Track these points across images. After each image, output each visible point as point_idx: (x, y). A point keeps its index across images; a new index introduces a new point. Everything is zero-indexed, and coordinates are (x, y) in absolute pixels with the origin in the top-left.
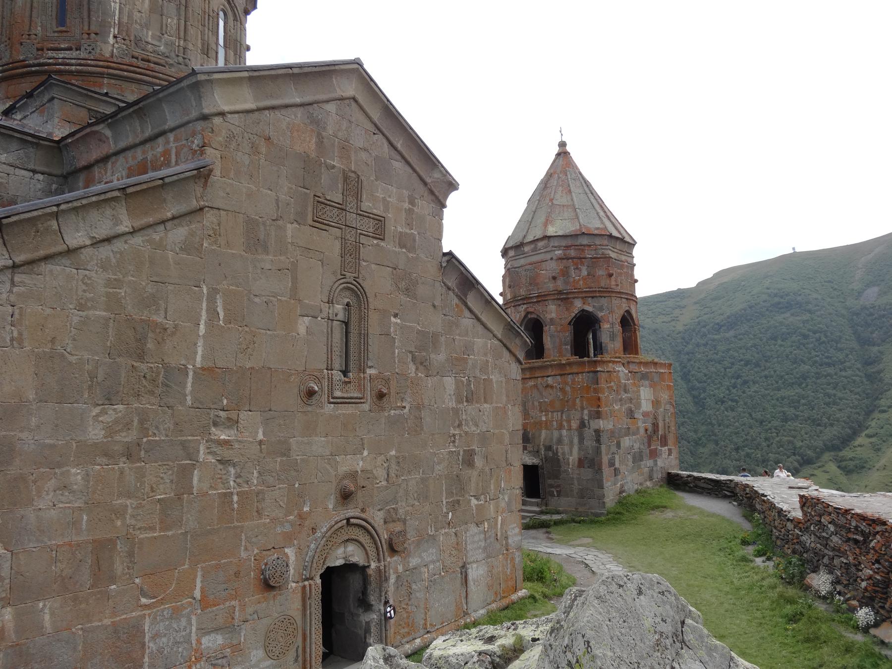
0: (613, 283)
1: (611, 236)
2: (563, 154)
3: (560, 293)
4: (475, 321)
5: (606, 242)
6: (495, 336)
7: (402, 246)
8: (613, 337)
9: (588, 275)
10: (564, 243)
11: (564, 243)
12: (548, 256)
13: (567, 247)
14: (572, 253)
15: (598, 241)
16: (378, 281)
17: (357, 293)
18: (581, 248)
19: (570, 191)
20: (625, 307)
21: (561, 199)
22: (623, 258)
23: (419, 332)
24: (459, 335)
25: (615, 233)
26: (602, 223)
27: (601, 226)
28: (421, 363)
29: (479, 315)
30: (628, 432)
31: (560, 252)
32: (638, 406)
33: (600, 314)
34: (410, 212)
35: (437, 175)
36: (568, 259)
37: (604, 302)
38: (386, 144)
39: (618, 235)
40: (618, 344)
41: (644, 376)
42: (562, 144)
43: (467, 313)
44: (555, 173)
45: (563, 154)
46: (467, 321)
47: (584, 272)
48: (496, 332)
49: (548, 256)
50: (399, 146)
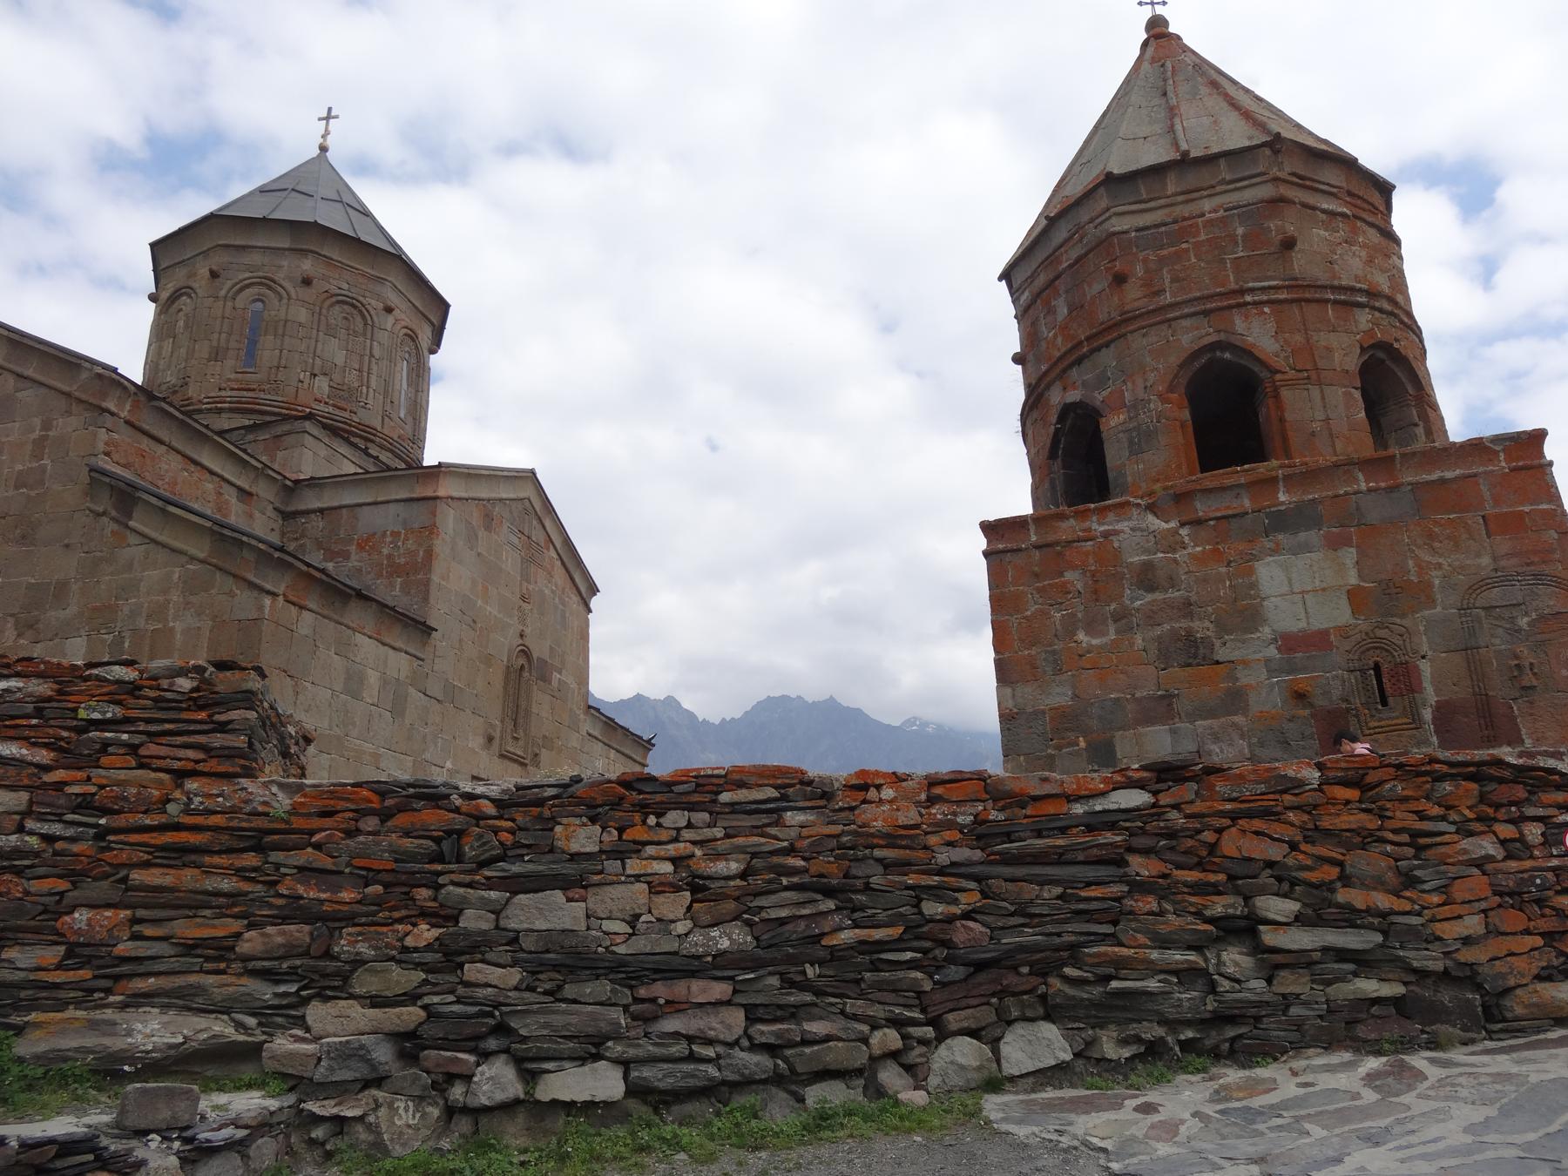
4: (152, 546)
6: (193, 559)
7: (16, 488)
8: (1140, 441)
9: (1070, 312)
13: (1033, 277)
14: (1042, 279)
15: (1084, 215)
23: (30, 586)
24: (112, 574)
28: (31, 627)
29: (153, 534)
30: (1162, 708)
31: (1027, 294)
33: (1098, 397)
34: (44, 438)
35: (84, 375)
37: (1108, 358)
38: (11, 380)
41: (1281, 522)
43: (133, 539)
46: (135, 551)
47: (1063, 311)
48: (193, 551)
50: (29, 372)
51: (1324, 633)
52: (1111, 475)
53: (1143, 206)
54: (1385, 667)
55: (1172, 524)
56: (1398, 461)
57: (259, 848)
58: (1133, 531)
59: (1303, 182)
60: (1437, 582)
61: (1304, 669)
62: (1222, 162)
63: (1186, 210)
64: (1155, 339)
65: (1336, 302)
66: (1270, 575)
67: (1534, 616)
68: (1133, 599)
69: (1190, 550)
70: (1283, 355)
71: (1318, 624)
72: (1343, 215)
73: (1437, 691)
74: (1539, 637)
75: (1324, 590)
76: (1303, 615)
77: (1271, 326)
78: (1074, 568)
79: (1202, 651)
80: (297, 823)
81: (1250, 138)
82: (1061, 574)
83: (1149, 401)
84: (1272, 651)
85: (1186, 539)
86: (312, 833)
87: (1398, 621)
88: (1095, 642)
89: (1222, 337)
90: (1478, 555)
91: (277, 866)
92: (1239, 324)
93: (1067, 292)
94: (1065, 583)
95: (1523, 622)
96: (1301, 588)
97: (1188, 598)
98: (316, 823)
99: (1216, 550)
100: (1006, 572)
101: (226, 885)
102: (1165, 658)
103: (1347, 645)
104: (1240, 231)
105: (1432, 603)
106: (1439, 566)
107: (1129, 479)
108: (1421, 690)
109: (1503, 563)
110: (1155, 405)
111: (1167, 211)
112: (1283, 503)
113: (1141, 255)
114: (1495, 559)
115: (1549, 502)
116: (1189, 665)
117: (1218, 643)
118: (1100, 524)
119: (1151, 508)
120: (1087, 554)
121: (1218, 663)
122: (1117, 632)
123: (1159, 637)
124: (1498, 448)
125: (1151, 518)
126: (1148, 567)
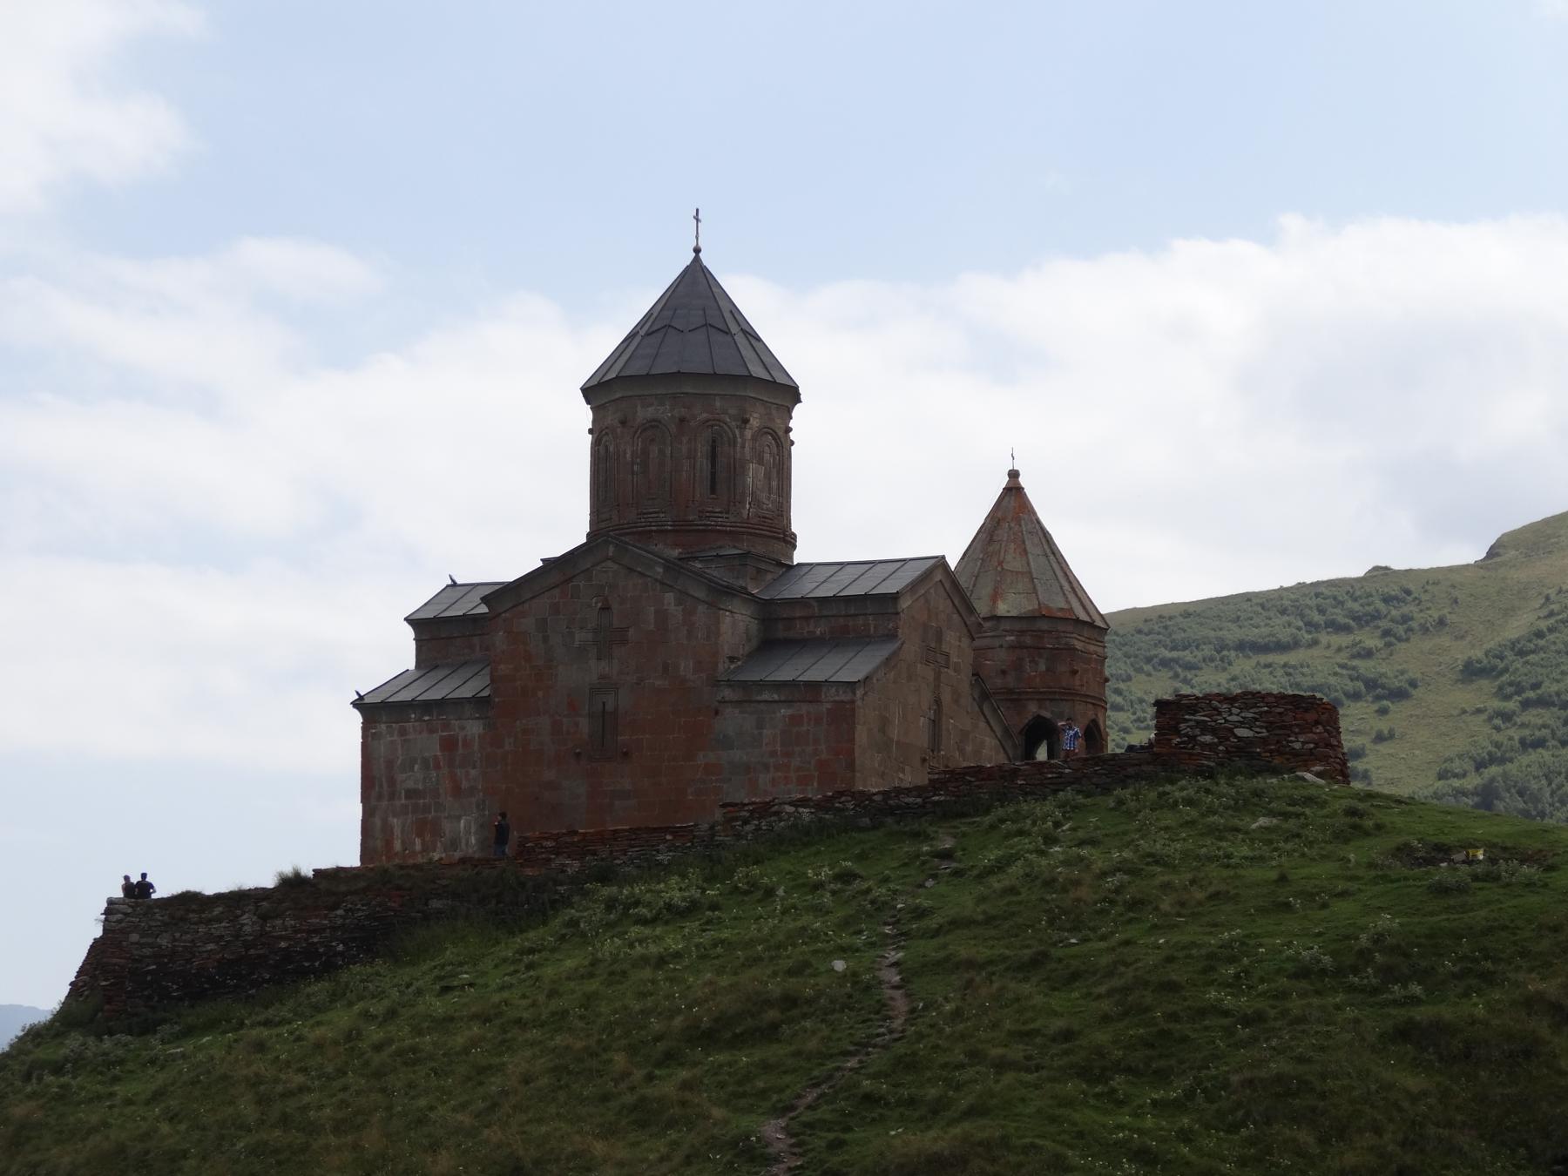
0: (1078, 683)
1: (1078, 621)
2: (1013, 490)
3: (1011, 691)
5: (1070, 628)
10: (1018, 626)
11: (1018, 626)
12: (997, 642)
13: (1022, 632)
14: (1028, 640)
16: (946, 697)
17: (938, 702)
19: (1025, 550)
20: (1091, 714)
21: (1013, 563)
22: (1092, 648)
25: (1083, 617)
26: (1068, 602)
27: (1063, 605)
36: (1022, 647)
39: (1087, 619)
42: (1014, 475)
44: (1004, 519)
45: (1013, 490)
46: (982, 724)
47: (1042, 667)
49: (997, 642)
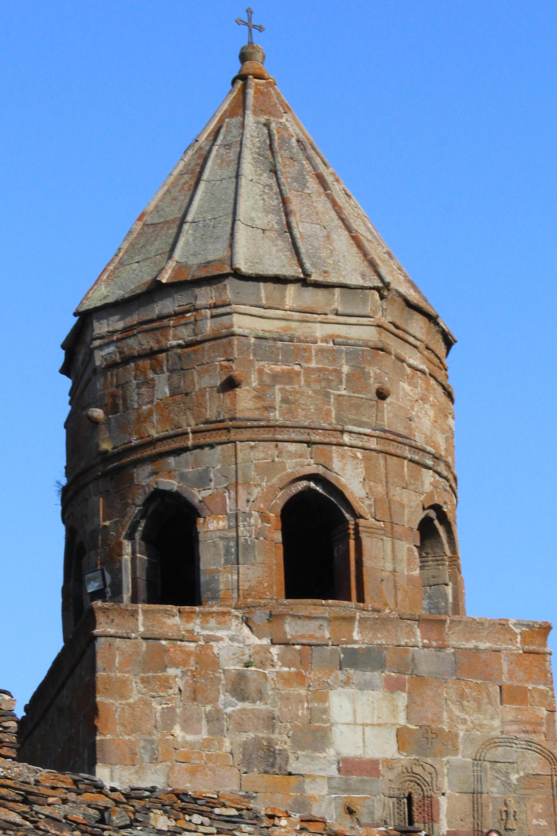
8: (236, 554)
9: (173, 395)
18: (157, 325)
32: (315, 736)
33: (198, 495)
40: (262, 569)
41: (353, 659)
51: (374, 763)
52: (203, 578)
53: (261, 311)
54: (415, 797)
55: (266, 641)
56: (447, 625)
57: (25, 801)
58: (230, 640)
59: (398, 331)
60: (461, 734)
61: (357, 791)
62: (337, 291)
63: (300, 330)
64: (262, 455)
65: (411, 461)
66: (343, 705)
67: (522, 774)
68: (226, 705)
69: (277, 669)
70: (367, 502)
71: (373, 753)
72: (423, 372)
73: (449, 823)
74: (523, 791)
75: (379, 725)
76: (361, 744)
77: (361, 470)
78: (176, 665)
79: (278, 761)
80: (43, 790)
81: (363, 276)
82: (164, 668)
83: (250, 515)
84: (333, 771)
85: (275, 658)
86: (48, 796)
87: (429, 760)
88: (190, 738)
89: (320, 470)
90: (492, 718)
91: (37, 813)
92: (336, 464)
93: (171, 371)
94: (167, 679)
95: (514, 777)
96: (361, 721)
97: (271, 712)
98: (50, 792)
99: (298, 674)
100: (114, 656)
101: (18, 819)
102: (248, 762)
103: (391, 775)
104: (345, 369)
105: (455, 751)
106: (464, 722)
107: (222, 587)
108: (438, 821)
109: (508, 728)
110: (255, 520)
111: (283, 324)
112: (355, 642)
113: (258, 365)
114: (503, 722)
115: (545, 684)
116: (266, 772)
117: (292, 757)
118: (203, 628)
119: (247, 621)
120: (189, 654)
121: (290, 774)
122: (210, 732)
123: (245, 743)
124: (517, 631)
125: (246, 630)
126: (241, 677)
